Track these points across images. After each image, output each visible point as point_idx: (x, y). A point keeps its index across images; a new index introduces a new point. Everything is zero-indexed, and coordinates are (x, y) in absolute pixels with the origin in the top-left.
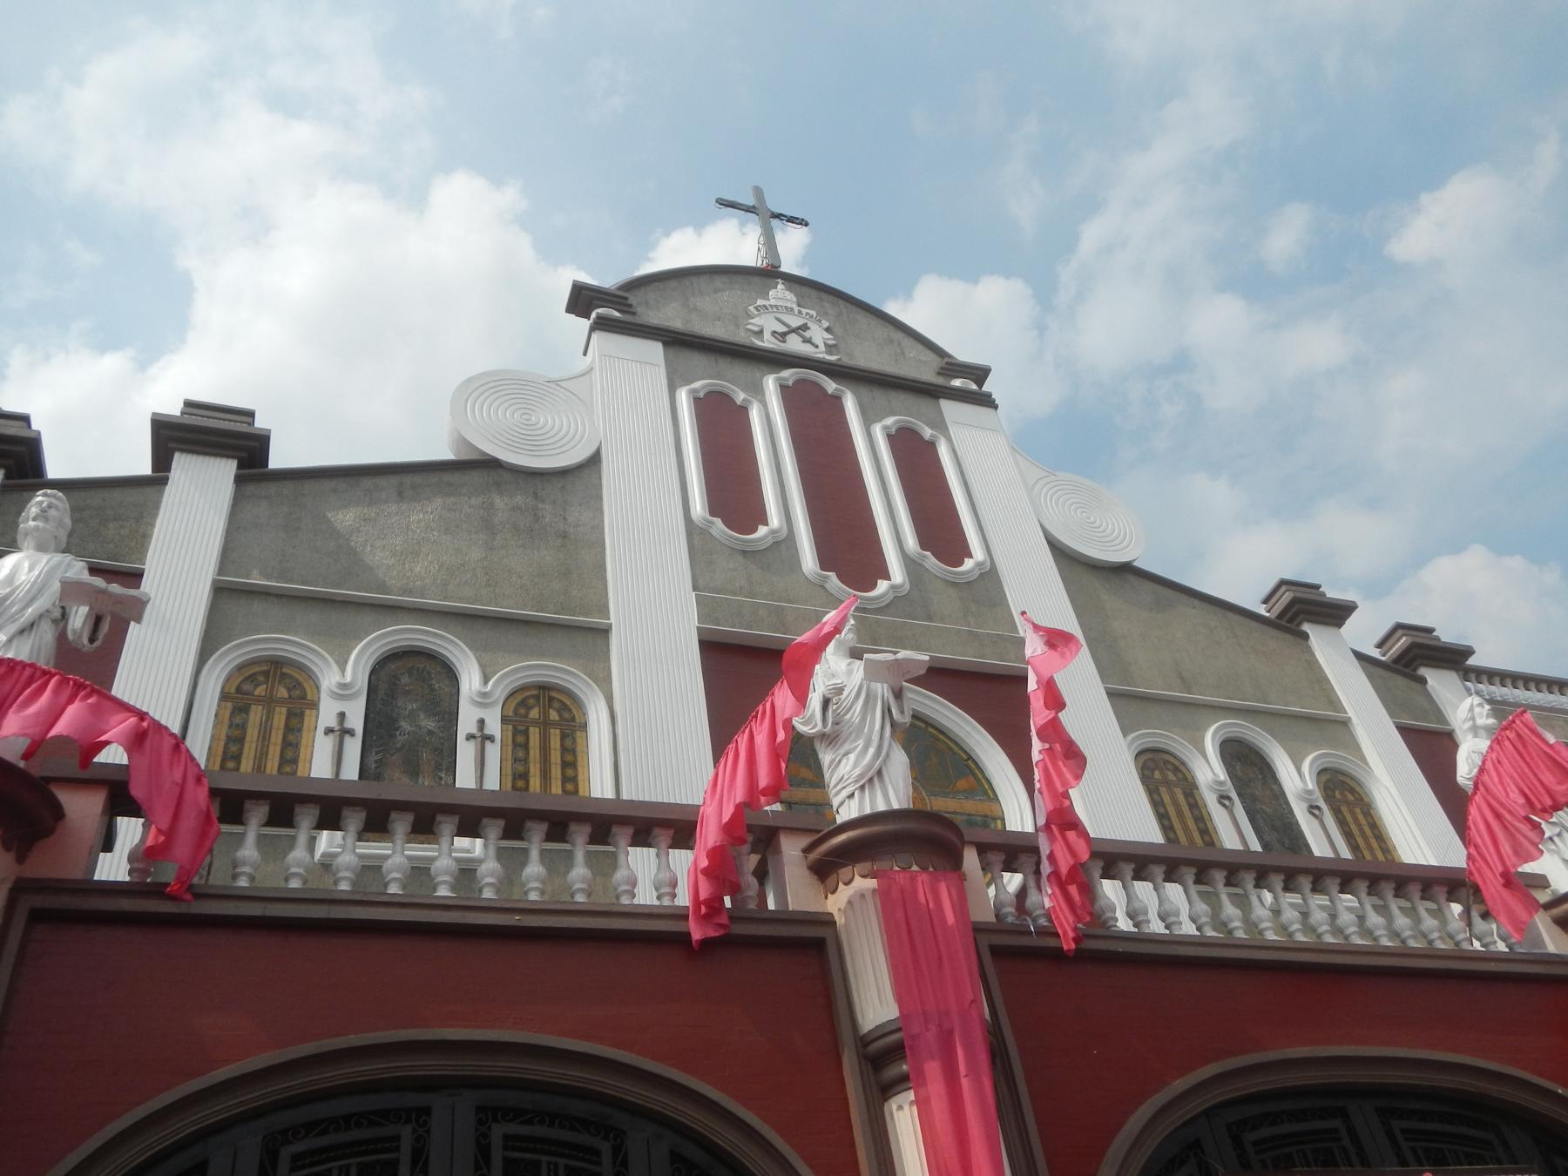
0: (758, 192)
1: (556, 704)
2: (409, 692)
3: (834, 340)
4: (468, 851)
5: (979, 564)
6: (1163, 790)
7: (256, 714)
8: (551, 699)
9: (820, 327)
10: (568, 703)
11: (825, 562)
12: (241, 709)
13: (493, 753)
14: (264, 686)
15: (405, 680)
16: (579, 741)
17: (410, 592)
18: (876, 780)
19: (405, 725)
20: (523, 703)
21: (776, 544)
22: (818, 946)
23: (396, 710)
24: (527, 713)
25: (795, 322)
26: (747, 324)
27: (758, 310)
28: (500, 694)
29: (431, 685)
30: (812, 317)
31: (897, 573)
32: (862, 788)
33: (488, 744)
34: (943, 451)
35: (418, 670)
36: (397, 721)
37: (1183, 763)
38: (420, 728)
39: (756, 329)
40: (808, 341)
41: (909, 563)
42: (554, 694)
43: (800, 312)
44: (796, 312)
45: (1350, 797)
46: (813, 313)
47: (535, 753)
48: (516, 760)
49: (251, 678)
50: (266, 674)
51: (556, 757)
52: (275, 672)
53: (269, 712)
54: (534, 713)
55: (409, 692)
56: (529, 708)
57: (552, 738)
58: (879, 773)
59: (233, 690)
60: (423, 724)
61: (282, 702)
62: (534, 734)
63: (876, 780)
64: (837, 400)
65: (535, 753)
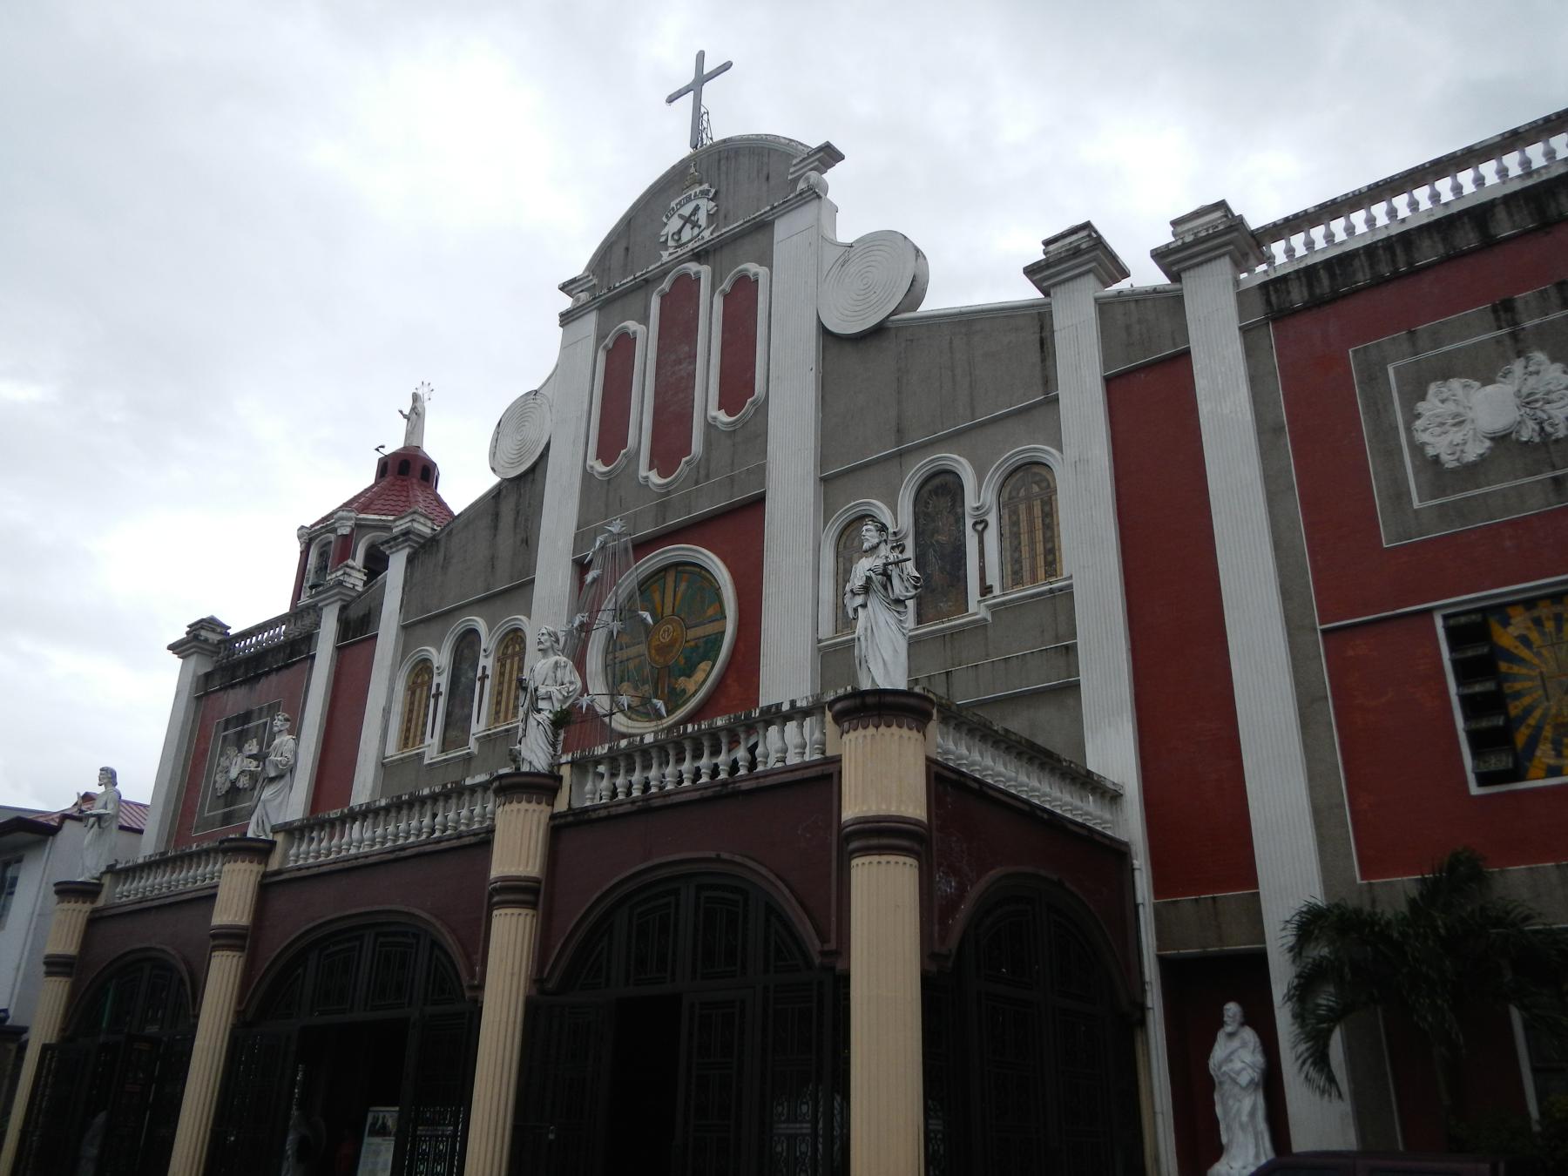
0: (701, 57)
1: (519, 640)
7: (418, 691)
12: (413, 693)
19: (463, 679)
20: (507, 647)
25: (687, 210)
27: (667, 216)
39: (663, 239)
40: (695, 225)
41: (710, 426)
45: (1036, 489)
46: (706, 186)
49: (417, 675)
59: (411, 684)
62: (508, 661)
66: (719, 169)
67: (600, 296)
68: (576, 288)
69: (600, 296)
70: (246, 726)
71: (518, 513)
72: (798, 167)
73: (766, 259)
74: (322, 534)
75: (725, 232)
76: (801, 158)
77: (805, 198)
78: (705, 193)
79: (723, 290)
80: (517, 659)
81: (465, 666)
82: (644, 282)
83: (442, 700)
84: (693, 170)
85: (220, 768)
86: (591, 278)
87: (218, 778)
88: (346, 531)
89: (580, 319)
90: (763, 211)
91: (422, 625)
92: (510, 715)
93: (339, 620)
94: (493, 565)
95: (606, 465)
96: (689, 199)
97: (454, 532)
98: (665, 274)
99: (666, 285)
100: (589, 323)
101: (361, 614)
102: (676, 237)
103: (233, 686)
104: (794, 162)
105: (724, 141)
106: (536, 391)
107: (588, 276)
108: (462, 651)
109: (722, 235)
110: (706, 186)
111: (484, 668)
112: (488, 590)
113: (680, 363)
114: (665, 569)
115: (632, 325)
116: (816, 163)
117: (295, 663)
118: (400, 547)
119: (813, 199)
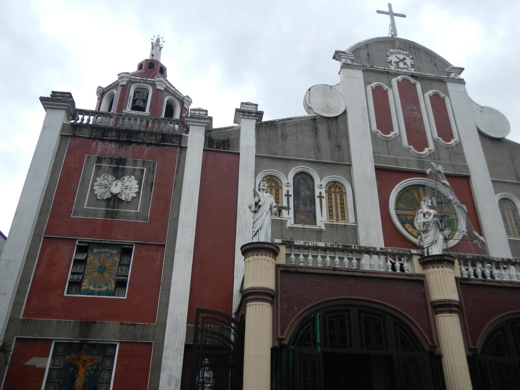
0: (390, 5)
1: (338, 187)
2: (302, 184)
3: (413, 62)
4: (320, 227)
5: (456, 141)
6: (506, 211)
8: (337, 186)
9: (409, 58)
10: (341, 186)
11: (409, 143)
13: (324, 201)
14: (269, 183)
15: (301, 181)
16: (344, 197)
17: (301, 157)
18: (435, 243)
20: (330, 187)
21: (396, 137)
22: (422, 282)
23: (300, 189)
24: (331, 189)
25: (401, 57)
26: (387, 59)
27: (390, 54)
28: (324, 185)
29: (307, 182)
30: (407, 54)
31: (432, 146)
32: (432, 245)
33: (322, 198)
34: (447, 100)
35: (304, 178)
36: (300, 192)
37: (513, 203)
38: (305, 193)
39: (389, 61)
40: (405, 64)
41: (435, 142)
42: (337, 184)
43: (403, 53)
44: (402, 54)
46: (407, 53)
47: (333, 201)
48: (329, 202)
50: (269, 179)
51: (339, 202)
52: (271, 179)
53: (271, 190)
54: (333, 190)
55: (302, 184)
56: (331, 188)
57: (337, 196)
58: (436, 241)
60: (306, 193)
61: (274, 187)
62: (333, 195)
63: (435, 243)
64: (414, 85)
65: (333, 201)
66: (410, 49)
67: (366, 66)
68: (344, 56)
69: (366, 66)
70: (121, 166)
71: (330, 133)
72: (450, 69)
73: (446, 92)
74: (140, 82)
75: (427, 75)
76: (452, 67)
77: (460, 82)
78: (409, 56)
79: (430, 95)
80: (338, 195)
81: (302, 188)
82: (386, 72)
83: (291, 199)
84: (397, 43)
85: (96, 184)
86: (352, 56)
87: (95, 188)
88: (162, 89)
89: (353, 70)
90: (444, 77)
91: (268, 159)
92: (340, 218)
93: (206, 137)
94: (318, 149)
95: (382, 133)
96: (400, 53)
97: (286, 125)
98: (396, 75)
99: (399, 78)
100: (359, 74)
101: (222, 139)
102: (397, 64)
103: (105, 140)
104: (450, 67)
105: (413, 42)
106: (331, 87)
107: (351, 55)
108: (298, 181)
109: (426, 75)
110: (407, 53)
111: (320, 193)
112: (318, 159)
113: (413, 111)
114: (418, 186)
115: (386, 87)
116: (458, 72)
117: (165, 145)
118: (251, 118)
119: (463, 84)
